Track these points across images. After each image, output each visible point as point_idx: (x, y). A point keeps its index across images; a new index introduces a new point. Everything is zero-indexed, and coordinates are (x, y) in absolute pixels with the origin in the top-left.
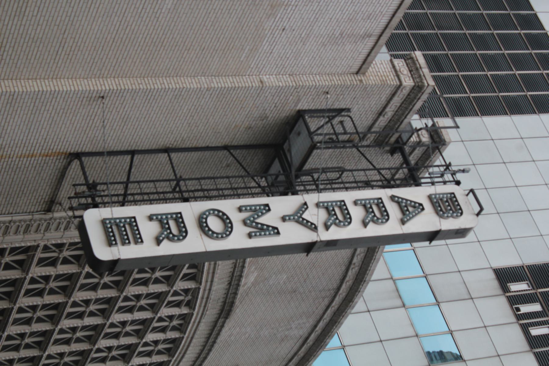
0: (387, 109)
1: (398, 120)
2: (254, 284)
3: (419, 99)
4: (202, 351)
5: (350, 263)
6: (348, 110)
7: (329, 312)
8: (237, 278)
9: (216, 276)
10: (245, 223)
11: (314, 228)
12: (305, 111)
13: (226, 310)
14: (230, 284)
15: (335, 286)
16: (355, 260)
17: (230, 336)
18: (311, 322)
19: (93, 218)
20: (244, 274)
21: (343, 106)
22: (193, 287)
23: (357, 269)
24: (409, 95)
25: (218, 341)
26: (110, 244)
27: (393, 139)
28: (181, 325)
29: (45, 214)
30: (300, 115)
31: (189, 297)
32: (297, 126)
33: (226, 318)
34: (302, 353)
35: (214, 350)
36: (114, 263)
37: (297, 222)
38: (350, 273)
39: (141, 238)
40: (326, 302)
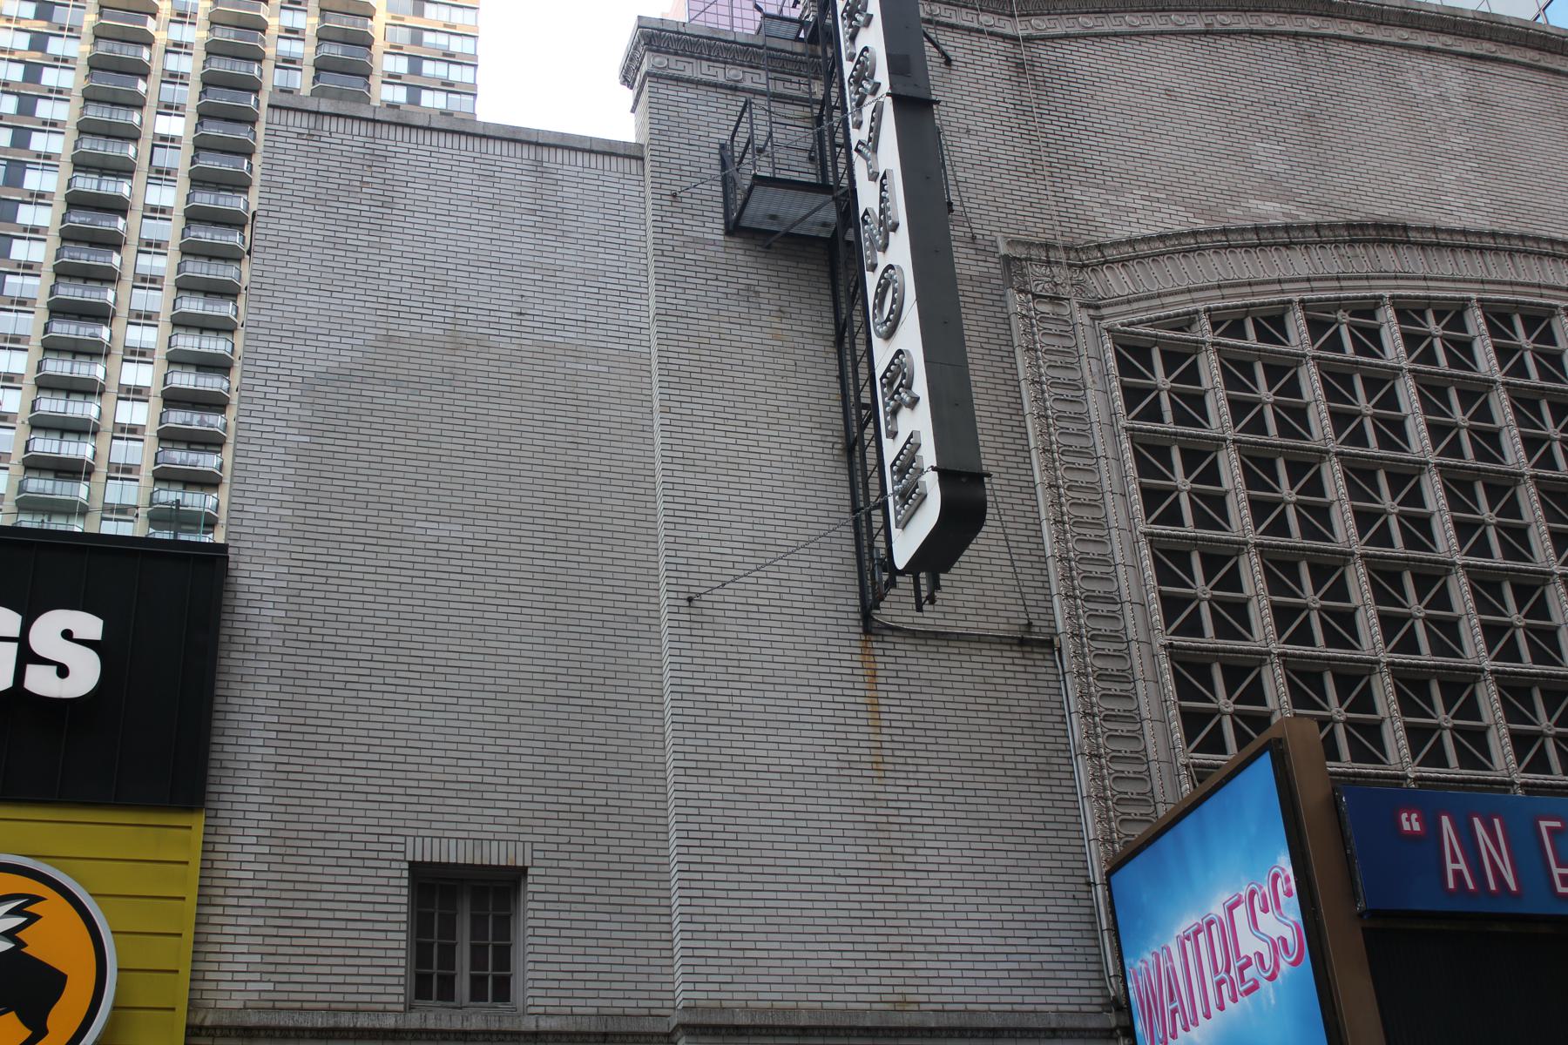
0: (721, 79)
1: (745, 53)
2: (1287, 197)
3: (678, 33)
4: (1527, 253)
5: (1206, 33)
6: (723, 147)
7: (1378, 34)
8: (1267, 235)
9: (1262, 276)
10: (885, 247)
11: (878, 111)
12: (726, 224)
13: (1389, 234)
14: (1287, 246)
15: (1286, 44)
16: (1199, 26)
17: (1472, 208)
18: (1409, 62)
19: (905, 545)
20: (1249, 224)
21: (715, 160)
22: (1299, 314)
23: (1220, 17)
24: (676, 54)
25: (1488, 227)
26: (924, 497)
27: (799, 48)
28: (1439, 316)
29: (1060, 650)
30: (734, 229)
31: (1344, 317)
32: (764, 227)
33: (1405, 228)
34: (1530, 56)
35: (1516, 229)
36: (944, 474)
37: (875, 150)
38: (1242, 26)
39: (908, 442)
40: (1345, 48)
